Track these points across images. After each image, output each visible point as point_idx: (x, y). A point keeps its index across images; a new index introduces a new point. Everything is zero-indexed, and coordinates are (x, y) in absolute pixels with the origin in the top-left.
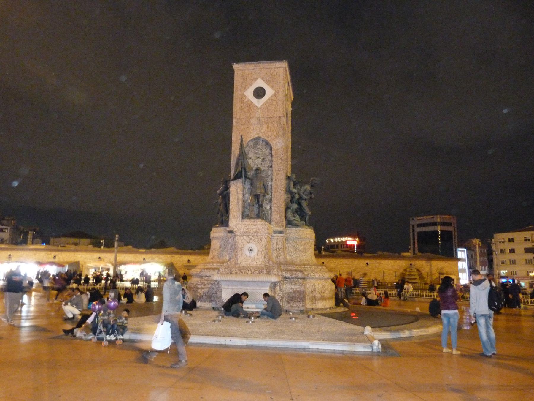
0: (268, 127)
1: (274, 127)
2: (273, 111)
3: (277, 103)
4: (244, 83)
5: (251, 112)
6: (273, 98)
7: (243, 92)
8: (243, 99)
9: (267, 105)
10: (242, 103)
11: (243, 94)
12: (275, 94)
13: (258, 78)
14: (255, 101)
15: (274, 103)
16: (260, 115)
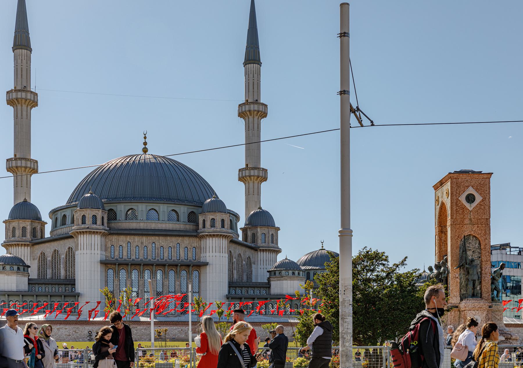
0: (478, 227)
1: (483, 227)
2: (482, 214)
3: (484, 207)
4: (458, 190)
5: (464, 214)
6: (481, 203)
7: (457, 197)
8: (458, 203)
9: (477, 209)
10: (457, 206)
11: (458, 199)
12: (483, 200)
13: (469, 187)
14: (467, 205)
15: (482, 207)
16: (472, 216)
